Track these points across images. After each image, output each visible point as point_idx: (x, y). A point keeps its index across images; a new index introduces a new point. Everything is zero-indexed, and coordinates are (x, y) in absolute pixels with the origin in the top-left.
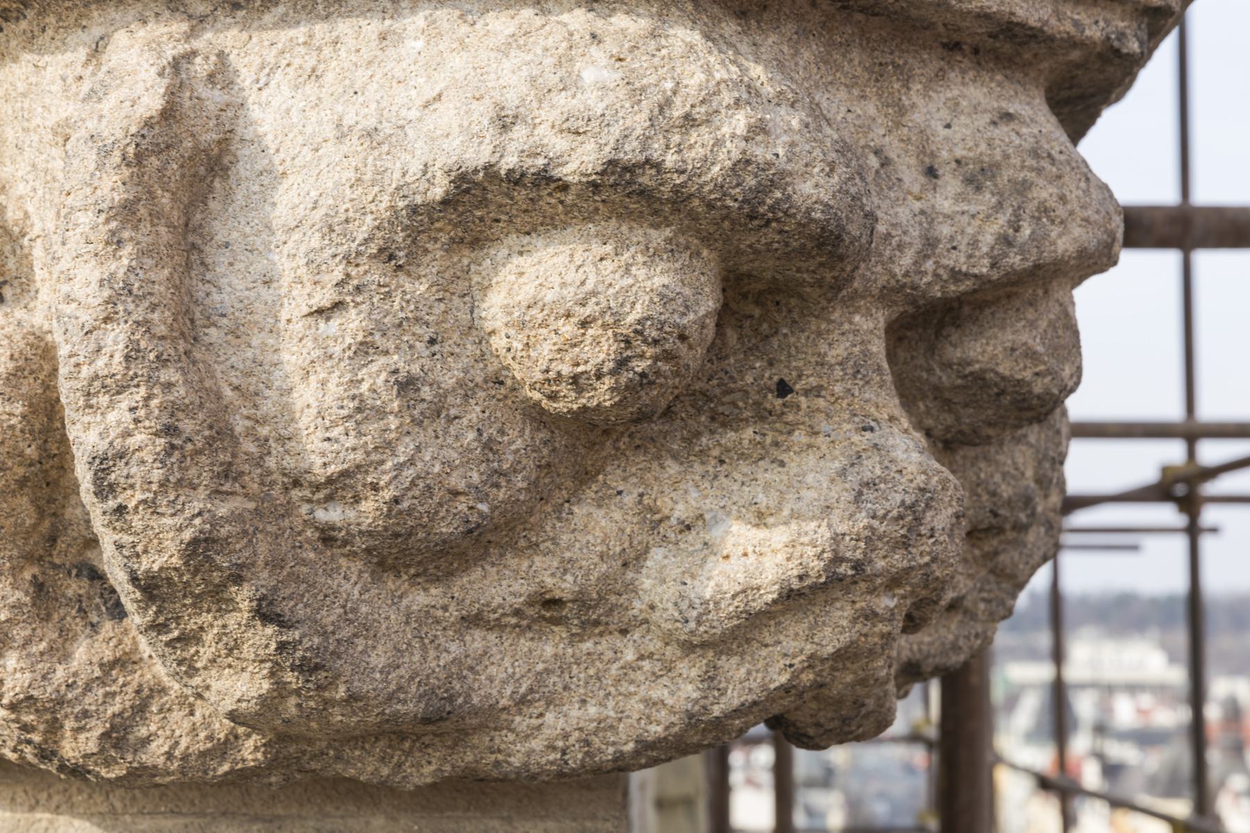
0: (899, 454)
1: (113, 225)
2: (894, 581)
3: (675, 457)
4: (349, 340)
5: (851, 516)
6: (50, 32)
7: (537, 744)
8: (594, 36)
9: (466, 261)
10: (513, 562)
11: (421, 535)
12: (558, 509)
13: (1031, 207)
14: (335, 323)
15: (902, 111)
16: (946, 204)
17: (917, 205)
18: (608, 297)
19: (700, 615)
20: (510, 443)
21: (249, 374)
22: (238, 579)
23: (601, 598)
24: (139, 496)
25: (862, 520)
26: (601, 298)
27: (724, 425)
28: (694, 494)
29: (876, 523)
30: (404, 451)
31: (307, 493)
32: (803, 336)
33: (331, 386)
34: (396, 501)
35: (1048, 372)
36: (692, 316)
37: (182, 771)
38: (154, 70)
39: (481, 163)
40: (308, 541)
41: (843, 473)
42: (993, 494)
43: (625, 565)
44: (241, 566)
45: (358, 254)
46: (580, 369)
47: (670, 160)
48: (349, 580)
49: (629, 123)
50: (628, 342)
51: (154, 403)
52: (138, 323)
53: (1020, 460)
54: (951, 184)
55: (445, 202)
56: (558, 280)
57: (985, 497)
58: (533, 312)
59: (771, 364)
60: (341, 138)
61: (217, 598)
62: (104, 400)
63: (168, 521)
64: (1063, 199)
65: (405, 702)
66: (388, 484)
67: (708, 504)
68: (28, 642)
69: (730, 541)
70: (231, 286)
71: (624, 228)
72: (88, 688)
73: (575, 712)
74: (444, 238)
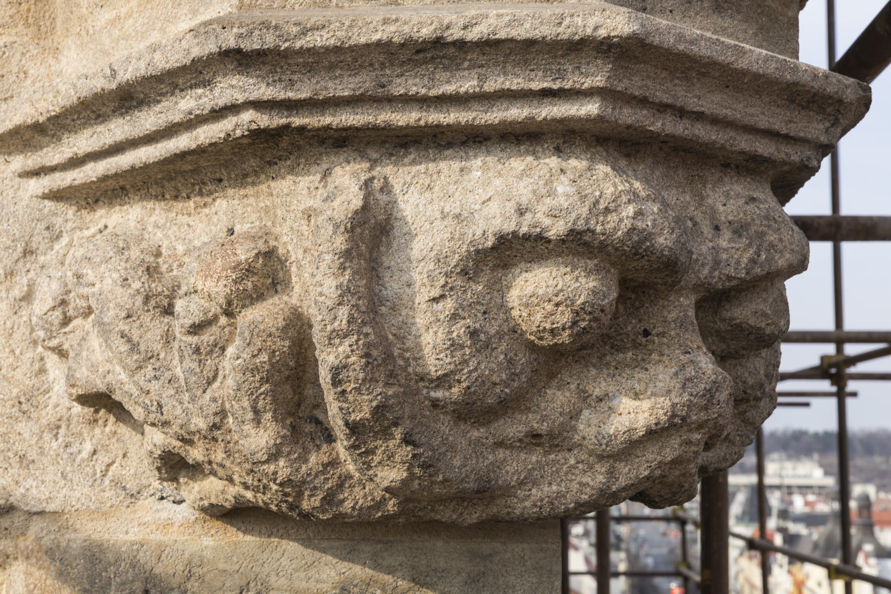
0: (703, 365)
1: (342, 260)
2: (700, 426)
3: (594, 366)
4: (447, 313)
5: (680, 395)
6: (302, 166)
7: (527, 504)
8: (562, 170)
9: (500, 275)
10: (519, 417)
11: (479, 404)
12: (540, 391)
13: (766, 244)
14: (441, 305)
15: (702, 198)
16: (724, 244)
17: (711, 244)
18: (568, 293)
19: (608, 442)
20: (520, 360)
21: (401, 328)
22: (396, 425)
23: (560, 434)
24: (353, 386)
25: (686, 397)
26: (565, 292)
27: (617, 350)
28: (604, 384)
29: (692, 398)
30: (472, 364)
31: (427, 384)
32: (656, 308)
33: (439, 334)
34: (469, 388)
35: (773, 323)
36: (607, 301)
37: (359, 516)
38: (357, 187)
39: (511, 230)
40: (426, 406)
41: (676, 374)
42: (745, 382)
43: (571, 418)
44: (398, 418)
45: (451, 272)
46: (554, 326)
47: (599, 228)
48: (444, 426)
49: (579, 212)
50: (577, 313)
51: (361, 342)
52: (353, 306)
53: (757, 365)
54: (727, 234)
55: (493, 248)
56: (545, 284)
57: (740, 384)
58: (533, 299)
59: (640, 321)
60: (443, 218)
61: (386, 434)
62: (337, 341)
63: (366, 397)
64: (781, 240)
65: (468, 483)
66: (465, 380)
67: (611, 388)
68: (289, 453)
69: (622, 406)
70: (392, 287)
71: (575, 260)
72: (316, 476)
73: (546, 489)
74: (491, 264)
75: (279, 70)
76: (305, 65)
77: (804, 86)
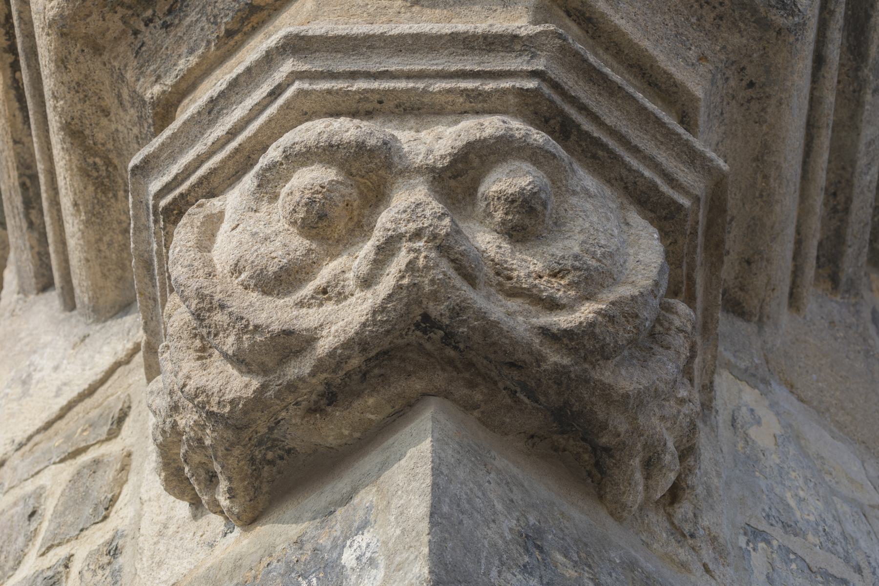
2: (417, 235)
55: (259, 186)
77: (465, 33)
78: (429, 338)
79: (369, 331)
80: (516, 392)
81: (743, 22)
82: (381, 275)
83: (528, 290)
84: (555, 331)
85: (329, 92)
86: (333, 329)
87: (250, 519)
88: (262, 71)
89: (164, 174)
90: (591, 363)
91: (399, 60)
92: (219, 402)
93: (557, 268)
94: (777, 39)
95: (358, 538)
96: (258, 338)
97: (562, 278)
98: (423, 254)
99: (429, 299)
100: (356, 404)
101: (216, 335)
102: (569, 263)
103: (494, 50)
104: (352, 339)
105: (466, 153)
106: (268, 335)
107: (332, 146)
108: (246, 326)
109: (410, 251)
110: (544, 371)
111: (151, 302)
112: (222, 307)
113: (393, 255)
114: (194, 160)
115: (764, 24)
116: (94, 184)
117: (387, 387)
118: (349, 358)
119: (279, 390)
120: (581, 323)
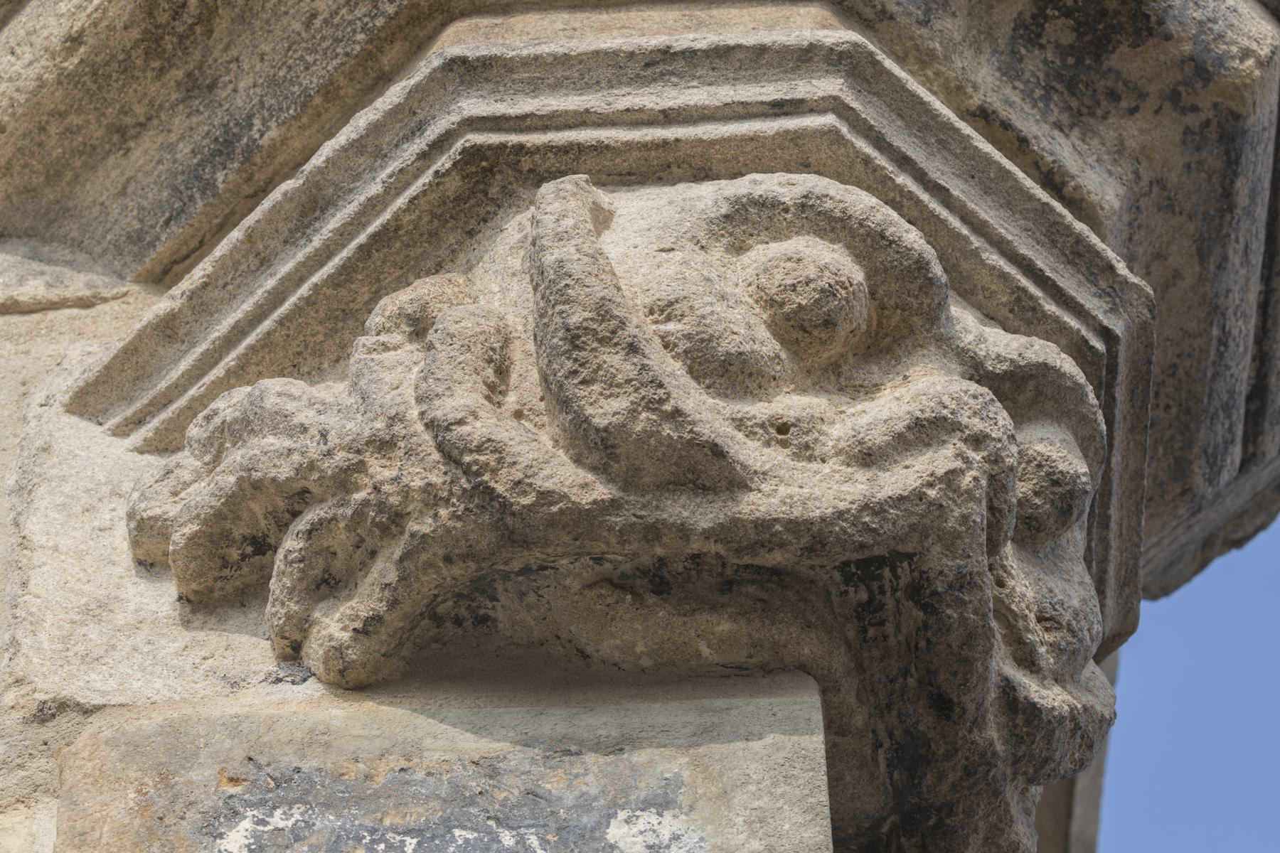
2: (977, 441)
42: (1051, 591)
55: (726, 216)
57: (1045, 590)
75: (501, 89)
76: (531, 82)
78: (846, 592)
79: (844, 531)
80: (881, 746)
81: (1165, 449)
82: (896, 462)
83: (1015, 615)
84: (1022, 694)
85: (867, 160)
86: (783, 490)
87: (353, 682)
88: (779, 65)
89: (502, 100)
90: (1015, 774)
91: (964, 187)
92: (519, 482)
93: (1050, 612)
94: (1173, 500)
95: (648, 819)
96: (667, 430)
97: (1047, 630)
98: (973, 473)
99: (940, 539)
100: (704, 618)
101: (584, 382)
102: (1067, 617)
103: (1075, 265)
104: (810, 522)
105: (1032, 375)
106: (687, 436)
107: (883, 237)
108: (661, 401)
109: (960, 455)
110: (972, 743)
111: (254, 262)
112: (633, 349)
113: (928, 445)
114: (575, 112)
115: (1181, 469)
116: (146, 31)
117: (767, 622)
118: (782, 545)
119: (633, 525)
120: (1053, 708)
